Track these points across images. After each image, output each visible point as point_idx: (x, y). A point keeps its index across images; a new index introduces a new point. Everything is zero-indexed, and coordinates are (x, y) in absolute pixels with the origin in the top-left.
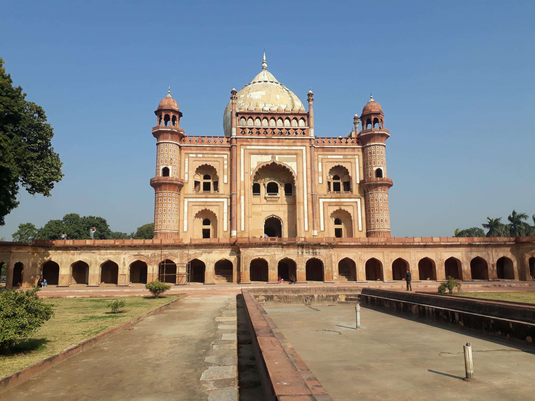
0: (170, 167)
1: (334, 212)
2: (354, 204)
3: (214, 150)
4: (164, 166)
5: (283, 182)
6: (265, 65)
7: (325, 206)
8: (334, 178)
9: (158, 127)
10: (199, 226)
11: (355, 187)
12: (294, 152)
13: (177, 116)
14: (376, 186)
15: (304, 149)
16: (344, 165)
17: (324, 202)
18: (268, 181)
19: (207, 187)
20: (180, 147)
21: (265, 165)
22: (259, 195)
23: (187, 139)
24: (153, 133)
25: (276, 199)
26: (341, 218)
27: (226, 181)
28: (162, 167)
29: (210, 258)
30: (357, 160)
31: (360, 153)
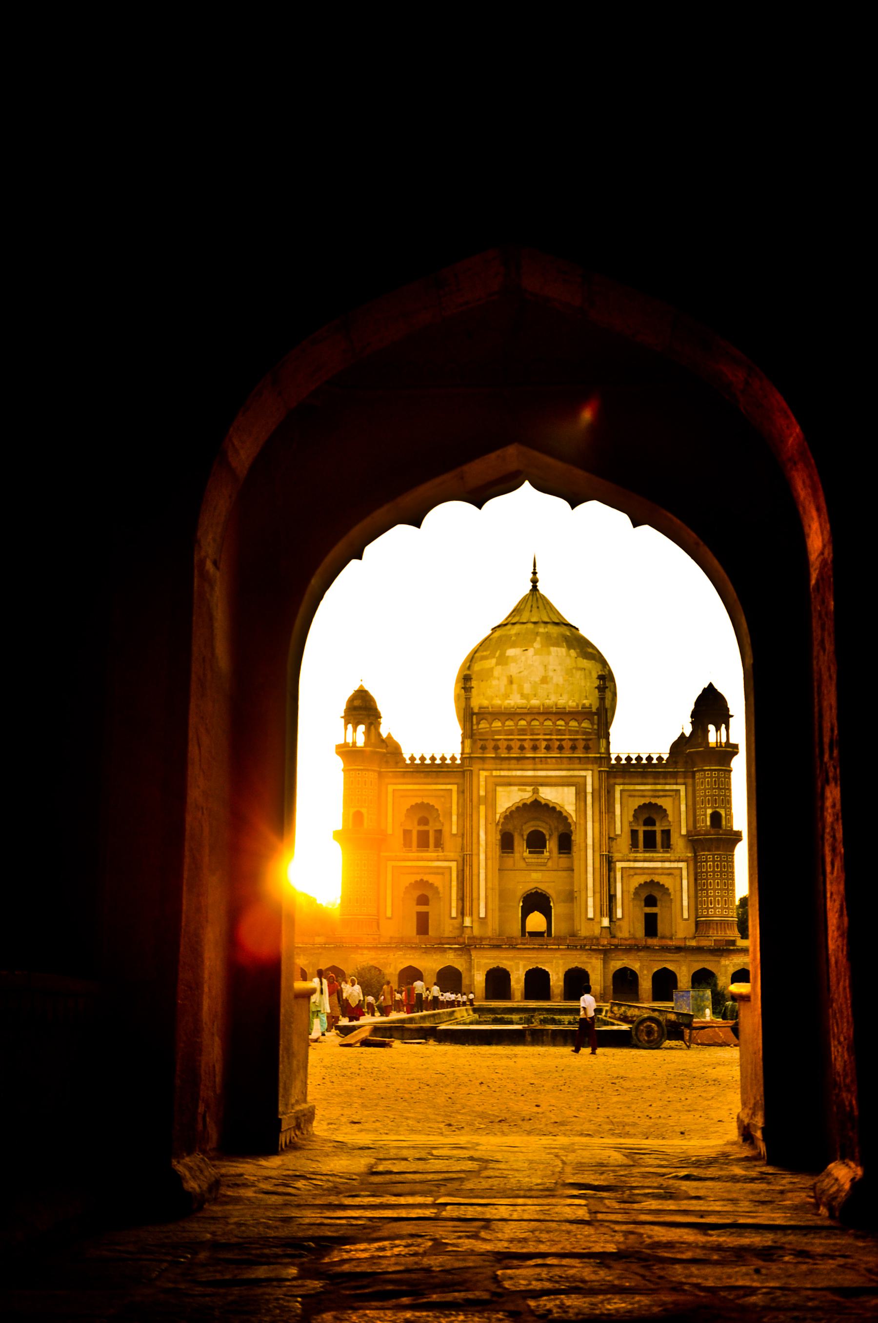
0: (364, 810)
1: (640, 885)
2: (678, 871)
3: (437, 777)
4: (356, 809)
5: (557, 828)
7: (624, 875)
9: (346, 745)
11: (678, 843)
15: (589, 777)
16: (659, 802)
18: (528, 829)
20: (380, 773)
22: (512, 853)
25: (543, 861)
26: (657, 895)
27: (454, 831)
28: (353, 810)
30: (683, 794)
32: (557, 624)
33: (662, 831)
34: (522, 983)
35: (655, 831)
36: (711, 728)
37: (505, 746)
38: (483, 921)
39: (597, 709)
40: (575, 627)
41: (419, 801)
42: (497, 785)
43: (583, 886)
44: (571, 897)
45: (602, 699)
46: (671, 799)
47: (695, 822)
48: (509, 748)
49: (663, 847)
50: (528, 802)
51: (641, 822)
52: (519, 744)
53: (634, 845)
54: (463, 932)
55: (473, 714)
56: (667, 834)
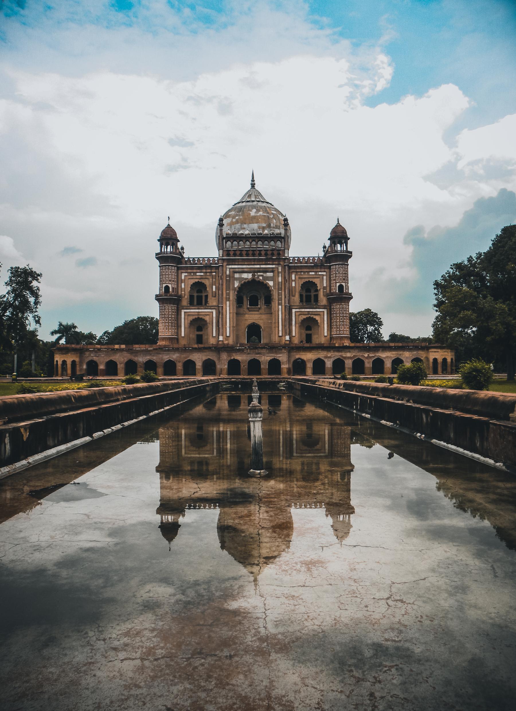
0: (170, 286)
11: (323, 300)
12: (271, 269)
20: (178, 267)
21: (247, 280)
28: (164, 285)
29: (199, 359)
33: (314, 295)
34: (246, 367)
35: (311, 295)
36: (339, 245)
40: (271, 204)
41: (197, 280)
43: (277, 322)
44: (272, 326)
45: (286, 230)
46: (319, 279)
49: (314, 302)
51: (304, 291)
53: (301, 301)
55: (224, 238)
56: (316, 297)
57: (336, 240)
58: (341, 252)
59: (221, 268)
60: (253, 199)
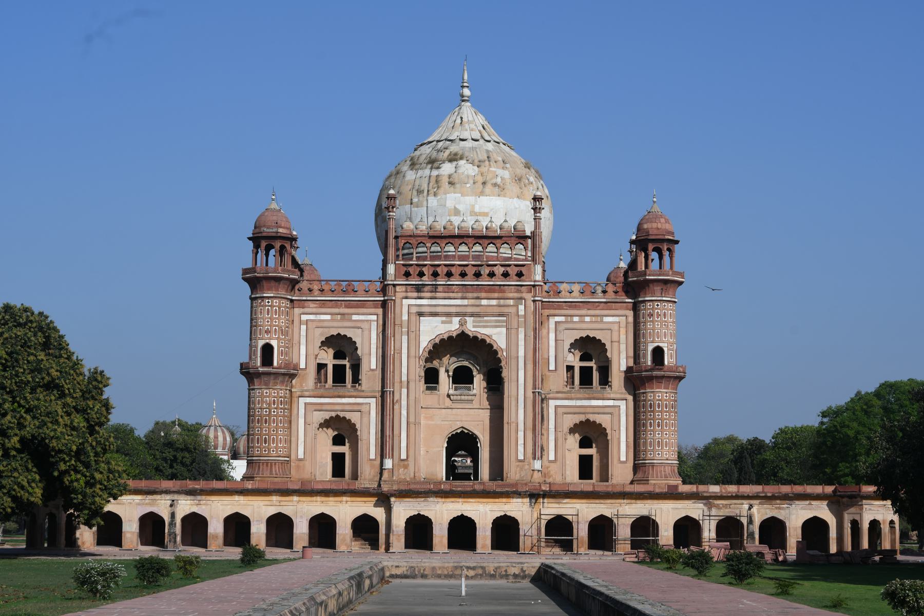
0: (274, 343)
1: (575, 425)
6: (467, 92)
8: (582, 359)
9: (253, 270)
10: (325, 449)
13: (288, 246)
14: (651, 379)
16: (598, 335)
17: (556, 407)
19: (339, 376)
23: (304, 285)
24: (244, 279)
25: (470, 398)
26: (591, 435)
27: (373, 366)
28: (261, 343)
31: (630, 314)
32: (489, 141)
36: (654, 255)
37: (431, 272)
38: (404, 463)
39: (533, 233)
42: (421, 314)
47: (636, 357)
48: (435, 275)
50: (454, 335)
52: (445, 270)
54: (381, 474)
57: (651, 247)
58: (660, 275)
59: (390, 304)
60: (465, 135)
